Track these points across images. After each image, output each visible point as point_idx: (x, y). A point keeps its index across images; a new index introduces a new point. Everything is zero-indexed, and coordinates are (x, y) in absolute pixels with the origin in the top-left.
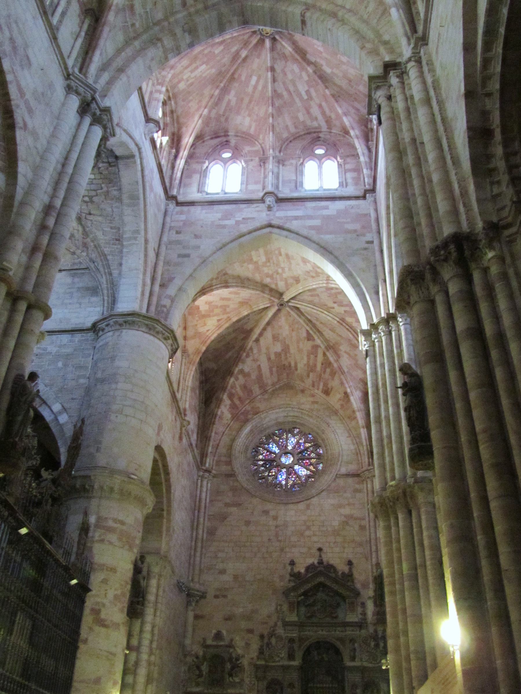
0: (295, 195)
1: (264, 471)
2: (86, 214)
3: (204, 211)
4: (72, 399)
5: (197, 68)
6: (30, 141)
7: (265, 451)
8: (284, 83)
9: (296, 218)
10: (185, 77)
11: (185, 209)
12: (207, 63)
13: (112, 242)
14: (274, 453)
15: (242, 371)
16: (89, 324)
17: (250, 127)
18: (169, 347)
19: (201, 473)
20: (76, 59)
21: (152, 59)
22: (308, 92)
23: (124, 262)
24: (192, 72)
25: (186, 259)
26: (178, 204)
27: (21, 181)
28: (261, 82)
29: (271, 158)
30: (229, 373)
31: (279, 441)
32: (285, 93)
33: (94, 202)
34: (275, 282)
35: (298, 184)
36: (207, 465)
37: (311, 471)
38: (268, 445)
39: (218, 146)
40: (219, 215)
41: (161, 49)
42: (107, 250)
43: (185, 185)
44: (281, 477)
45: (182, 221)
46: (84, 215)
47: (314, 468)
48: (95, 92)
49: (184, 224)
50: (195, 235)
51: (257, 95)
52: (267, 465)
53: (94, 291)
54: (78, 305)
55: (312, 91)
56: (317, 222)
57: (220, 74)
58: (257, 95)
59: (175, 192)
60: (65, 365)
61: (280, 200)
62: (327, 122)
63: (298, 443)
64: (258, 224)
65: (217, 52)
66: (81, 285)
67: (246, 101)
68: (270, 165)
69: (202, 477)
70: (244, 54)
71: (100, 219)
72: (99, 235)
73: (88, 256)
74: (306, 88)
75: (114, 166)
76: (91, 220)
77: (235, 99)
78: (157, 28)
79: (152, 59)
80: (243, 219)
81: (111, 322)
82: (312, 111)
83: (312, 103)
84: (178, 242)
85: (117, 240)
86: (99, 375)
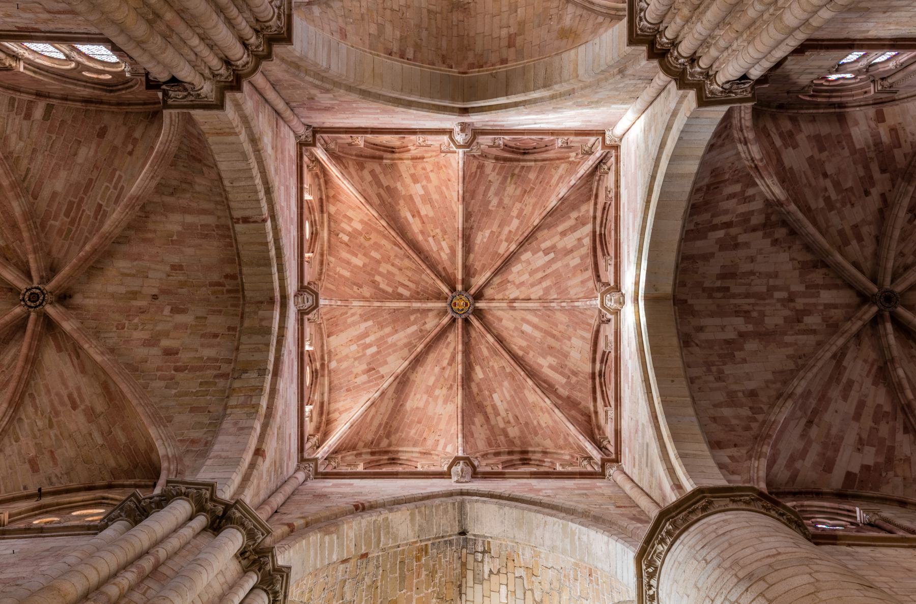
5: (494, 407)
8: (533, 285)
12: (492, 391)
17: (583, 338)
22: (546, 252)
24: (497, 414)
28: (530, 317)
32: (545, 284)
34: (821, 308)
51: (544, 325)
55: (544, 246)
58: (544, 325)
74: (541, 254)
82: (569, 246)
83: (560, 245)
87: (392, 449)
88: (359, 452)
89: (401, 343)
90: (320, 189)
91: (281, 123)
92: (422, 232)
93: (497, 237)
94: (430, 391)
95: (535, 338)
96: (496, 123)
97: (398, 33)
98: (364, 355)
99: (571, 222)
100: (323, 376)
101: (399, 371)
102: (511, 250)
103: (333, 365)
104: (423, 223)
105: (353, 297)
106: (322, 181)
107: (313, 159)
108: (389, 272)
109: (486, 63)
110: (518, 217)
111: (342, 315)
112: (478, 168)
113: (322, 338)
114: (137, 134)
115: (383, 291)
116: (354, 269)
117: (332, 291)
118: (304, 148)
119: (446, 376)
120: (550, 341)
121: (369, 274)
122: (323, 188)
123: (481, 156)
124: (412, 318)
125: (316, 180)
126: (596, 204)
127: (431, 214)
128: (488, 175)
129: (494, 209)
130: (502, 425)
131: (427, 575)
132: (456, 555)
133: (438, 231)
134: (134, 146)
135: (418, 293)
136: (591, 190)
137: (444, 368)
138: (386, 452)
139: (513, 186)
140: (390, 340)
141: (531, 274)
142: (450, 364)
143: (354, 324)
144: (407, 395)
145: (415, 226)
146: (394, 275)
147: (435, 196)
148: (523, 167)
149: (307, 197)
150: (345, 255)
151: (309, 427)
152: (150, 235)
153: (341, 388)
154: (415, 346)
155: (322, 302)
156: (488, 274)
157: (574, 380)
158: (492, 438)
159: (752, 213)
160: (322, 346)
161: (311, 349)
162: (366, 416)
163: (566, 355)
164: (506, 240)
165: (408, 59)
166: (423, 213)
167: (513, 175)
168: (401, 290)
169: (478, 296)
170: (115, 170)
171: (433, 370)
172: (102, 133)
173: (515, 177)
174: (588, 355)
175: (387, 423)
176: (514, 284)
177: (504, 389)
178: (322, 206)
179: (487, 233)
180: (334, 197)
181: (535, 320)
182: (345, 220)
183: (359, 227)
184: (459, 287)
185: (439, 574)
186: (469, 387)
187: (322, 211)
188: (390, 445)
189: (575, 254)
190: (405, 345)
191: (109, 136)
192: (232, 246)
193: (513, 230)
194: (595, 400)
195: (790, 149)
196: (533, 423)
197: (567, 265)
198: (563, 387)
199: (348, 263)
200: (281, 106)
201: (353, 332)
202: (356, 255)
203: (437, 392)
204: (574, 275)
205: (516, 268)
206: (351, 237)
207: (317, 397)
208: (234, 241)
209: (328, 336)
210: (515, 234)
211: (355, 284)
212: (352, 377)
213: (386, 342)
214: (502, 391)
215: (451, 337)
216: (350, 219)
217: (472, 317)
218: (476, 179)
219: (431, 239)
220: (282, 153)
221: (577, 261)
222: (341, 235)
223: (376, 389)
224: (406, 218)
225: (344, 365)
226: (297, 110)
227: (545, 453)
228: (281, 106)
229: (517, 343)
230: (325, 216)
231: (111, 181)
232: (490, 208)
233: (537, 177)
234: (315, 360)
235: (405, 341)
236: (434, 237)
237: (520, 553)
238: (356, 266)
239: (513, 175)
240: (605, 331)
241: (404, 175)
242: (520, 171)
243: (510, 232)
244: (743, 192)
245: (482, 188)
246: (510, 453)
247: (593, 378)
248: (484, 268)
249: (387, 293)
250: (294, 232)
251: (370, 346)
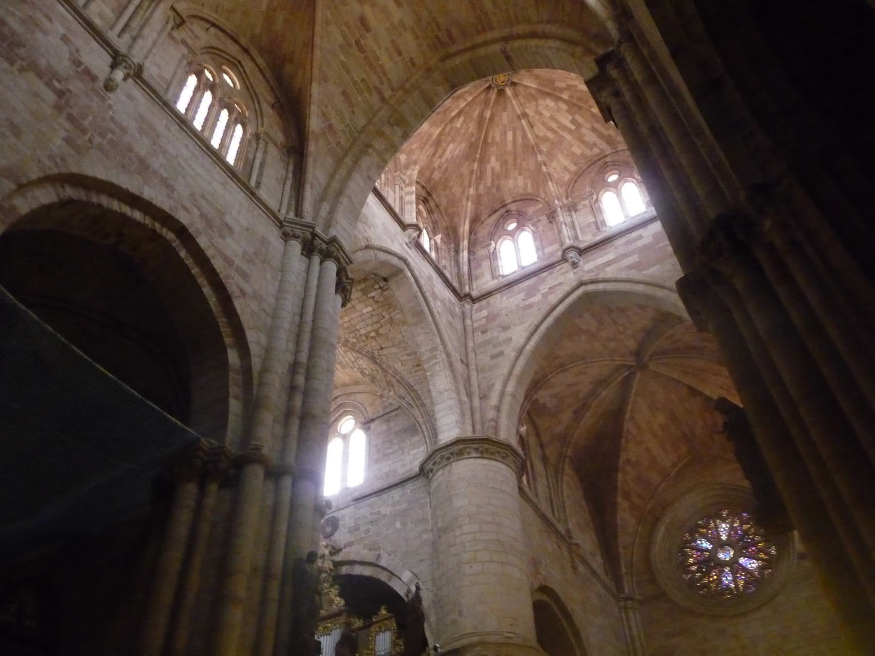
0: (599, 237)
1: (701, 578)
2: (378, 350)
3: (505, 298)
4: (421, 561)
5: (444, 151)
6: (254, 305)
7: (694, 552)
8: (543, 124)
9: (608, 264)
10: (436, 165)
11: (484, 303)
12: (453, 141)
13: (413, 370)
14: (707, 550)
15: (628, 461)
16: (417, 469)
17: (526, 185)
18: (512, 465)
19: (622, 603)
20: (289, 204)
21: (369, 168)
22: (573, 121)
23: (431, 387)
24: (441, 157)
25: (501, 359)
26: (474, 300)
27: (254, 348)
29: (559, 209)
30: (615, 469)
31: (708, 533)
32: (550, 135)
33: (381, 334)
35: (599, 225)
36: (627, 591)
37: (762, 559)
38: (695, 542)
39: (499, 220)
40: (522, 295)
41: (374, 154)
42: (411, 381)
43: (477, 278)
44: (727, 580)
45: (484, 318)
46: (376, 352)
47: (765, 555)
48: (313, 228)
49: (487, 320)
50: (502, 327)
52: (703, 568)
53: (413, 429)
54: (400, 452)
56: (634, 258)
57: (473, 146)
59: (467, 290)
60: (403, 524)
61: (582, 252)
62: (608, 143)
63: (732, 528)
64: (567, 288)
66: (397, 428)
67: (510, 161)
68: (562, 217)
69: (625, 608)
70: (488, 114)
71: (394, 350)
72: (398, 366)
73: (397, 394)
74: (570, 117)
75: (388, 289)
76: (386, 355)
77: (498, 164)
78: (363, 136)
79: (369, 168)
80: (549, 288)
81: (437, 459)
82: (586, 138)
83: (584, 131)
84: (488, 342)
85: (418, 366)
86: (440, 525)
93: (567, 78)
95: (506, 145)
176: (537, 107)
193: (578, 88)
197: (572, 145)
204: (567, 156)
205: (550, 102)
214: (457, 148)
217: (496, 91)
221: (577, 151)
229: (496, 134)
243: (576, 86)
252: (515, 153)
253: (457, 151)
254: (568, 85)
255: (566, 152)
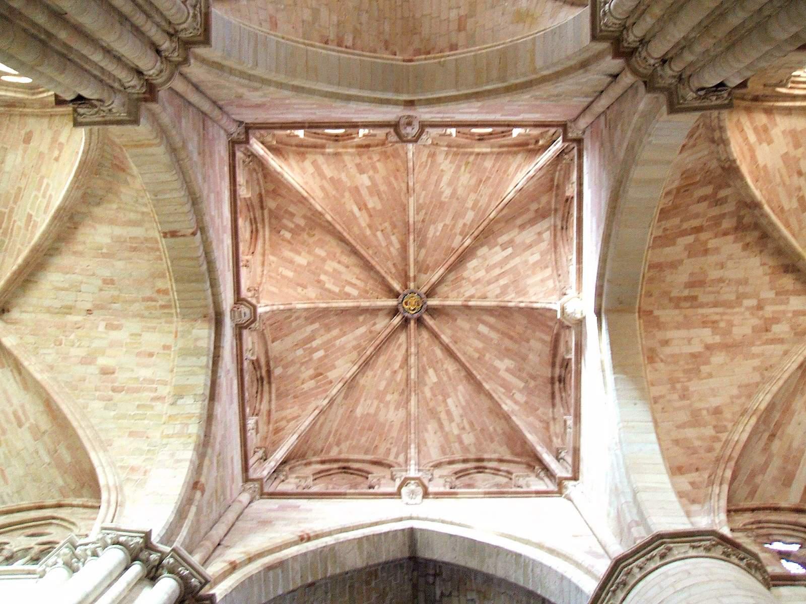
5: (448, 413)
8: (489, 283)
10: (456, 431)
12: (446, 396)
22: (504, 247)
24: (451, 420)
32: (502, 282)
51: (501, 325)
65: (434, 379)
82: (528, 241)
87: (342, 456)
88: (308, 461)
89: (349, 346)
90: (259, 184)
91: (209, 123)
92: (370, 226)
93: (451, 230)
94: (380, 396)
95: (492, 340)
96: (446, 115)
97: (335, 18)
98: (311, 360)
99: (530, 215)
100: (269, 383)
101: (348, 375)
102: (466, 244)
103: (278, 371)
104: (371, 216)
105: (296, 299)
106: (260, 175)
107: (249, 154)
108: (335, 270)
109: (433, 49)
110: (473, 208)
111: (286, 318)
112: (429, 156)
113: (266, 344)
114: (63, 139)
115: (330, 291)
116: (298, 269)
117: (273, 293)
118: (237, 147)
119: (398, 379)
120: (508, 343)
121: (314, 273)
122: (261, 181)
123: (432, 144)
124: (361, 318)
125: (254, 174)
126: (557, 195)
127: (379, 207)
128: (440, 164)
129: (447, 200)
130: (456, 431)
131: (377, 598)
132: (406, 577)
133: (387, 224)
134: (61, 151)
135: (367, 292)
136: (552, 180)
137: (395, 372)
138: (336, 461)
139: (468, 176)
140: (338, 342)
141: (487, 271)
142: (401, 367)
143: (299, 327)
144: (357, 401)
145: (363, 219)
146: (340, 273)
147: (383, 188)
148: (478, 154)
149: (244, 192)
150: (288, 254)
151: (253, 439)
152: (80, 248)
153: (287, 395)
154: (365, 349)
155: (260, 310)
156: (441, 271)
157: (532, 384)
158: (446, 446)
159: (723, 216)
160: (267, 352)
161: (254, 358)
162: (314, 424)
163: (524, 358)
164: (461, 234)
165: (346, 47)
166: (370, 205)
167: (467, 163)
168: (348, 289)
169: (420, 321)
170: (42, 178)
171: (383, 372)
172: (28, 139)
173: (470, 165)
174: (547, 358)
175: (337, 431)
177: (459, 394)
178: (261, 201)
179: (440, 226)
180: (274, 191)
181: (492, 320)
182: (287, 216)
183: (302, 222)
184: (412, 285)
185: (390, 596)
186: (423, 393)
187: (262, 208)
188: (340, 452)
189: (534, 249)
190: (355, 348)
191: (32, 144)
192: (161, 260)
193: (468, 223)
194: (554, 405)
195: (765, 145)
196: (488, 430)
197: (526, 262)
198: (520, 391)
199: (291, 262)
200: (206, 107)
201: (299, 336)
202: (299, 253)
203: (389, 397)
204: (534, 273)
205: (472, 264)
206: (293, 234)
207: (264, 407)
208: (162, 253)
209: (273, 342)
210: (471, 226)
211: (298, 285)
212: (298, 382)
213: (334, 346)
214: (457, 396)
215: (402, 337)
216: (292, 215)
218: (427, 168)
219: (379, 234)
220: (211, 156)
221: (537, 257)
222: (283, 232)
223: (324, 395)
224: (352, 212)
225: (291, 370)
226: (227, 109)
227: (501, 461)
228: (206, 107)
230: (266, 212)
231: (39, 190)
232: (443, 199)
233: (494, 166)
234: (260, 367)
235: (354, 343)
236: (382, 231)
237: (473, 578)
238: (300, 266)
239: (467, 163)
240: (565, 335)
241: (349, 165)
242: (476, 159)
244: (715, 193)
245: (434, 178)
246: (465, 461)
247: (553, 383)
248: (437, 265)
249: (333, 293)
250: (228, 241)
251: (317, 350)
252: (503, 333)
253: (461, 397)
254: (461, 234)
255: (529, 272)
